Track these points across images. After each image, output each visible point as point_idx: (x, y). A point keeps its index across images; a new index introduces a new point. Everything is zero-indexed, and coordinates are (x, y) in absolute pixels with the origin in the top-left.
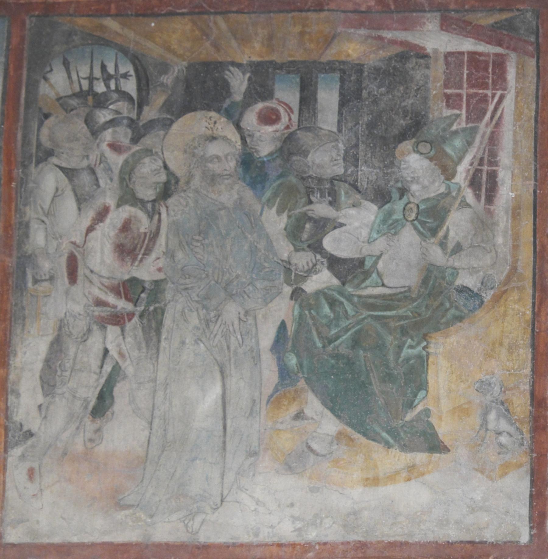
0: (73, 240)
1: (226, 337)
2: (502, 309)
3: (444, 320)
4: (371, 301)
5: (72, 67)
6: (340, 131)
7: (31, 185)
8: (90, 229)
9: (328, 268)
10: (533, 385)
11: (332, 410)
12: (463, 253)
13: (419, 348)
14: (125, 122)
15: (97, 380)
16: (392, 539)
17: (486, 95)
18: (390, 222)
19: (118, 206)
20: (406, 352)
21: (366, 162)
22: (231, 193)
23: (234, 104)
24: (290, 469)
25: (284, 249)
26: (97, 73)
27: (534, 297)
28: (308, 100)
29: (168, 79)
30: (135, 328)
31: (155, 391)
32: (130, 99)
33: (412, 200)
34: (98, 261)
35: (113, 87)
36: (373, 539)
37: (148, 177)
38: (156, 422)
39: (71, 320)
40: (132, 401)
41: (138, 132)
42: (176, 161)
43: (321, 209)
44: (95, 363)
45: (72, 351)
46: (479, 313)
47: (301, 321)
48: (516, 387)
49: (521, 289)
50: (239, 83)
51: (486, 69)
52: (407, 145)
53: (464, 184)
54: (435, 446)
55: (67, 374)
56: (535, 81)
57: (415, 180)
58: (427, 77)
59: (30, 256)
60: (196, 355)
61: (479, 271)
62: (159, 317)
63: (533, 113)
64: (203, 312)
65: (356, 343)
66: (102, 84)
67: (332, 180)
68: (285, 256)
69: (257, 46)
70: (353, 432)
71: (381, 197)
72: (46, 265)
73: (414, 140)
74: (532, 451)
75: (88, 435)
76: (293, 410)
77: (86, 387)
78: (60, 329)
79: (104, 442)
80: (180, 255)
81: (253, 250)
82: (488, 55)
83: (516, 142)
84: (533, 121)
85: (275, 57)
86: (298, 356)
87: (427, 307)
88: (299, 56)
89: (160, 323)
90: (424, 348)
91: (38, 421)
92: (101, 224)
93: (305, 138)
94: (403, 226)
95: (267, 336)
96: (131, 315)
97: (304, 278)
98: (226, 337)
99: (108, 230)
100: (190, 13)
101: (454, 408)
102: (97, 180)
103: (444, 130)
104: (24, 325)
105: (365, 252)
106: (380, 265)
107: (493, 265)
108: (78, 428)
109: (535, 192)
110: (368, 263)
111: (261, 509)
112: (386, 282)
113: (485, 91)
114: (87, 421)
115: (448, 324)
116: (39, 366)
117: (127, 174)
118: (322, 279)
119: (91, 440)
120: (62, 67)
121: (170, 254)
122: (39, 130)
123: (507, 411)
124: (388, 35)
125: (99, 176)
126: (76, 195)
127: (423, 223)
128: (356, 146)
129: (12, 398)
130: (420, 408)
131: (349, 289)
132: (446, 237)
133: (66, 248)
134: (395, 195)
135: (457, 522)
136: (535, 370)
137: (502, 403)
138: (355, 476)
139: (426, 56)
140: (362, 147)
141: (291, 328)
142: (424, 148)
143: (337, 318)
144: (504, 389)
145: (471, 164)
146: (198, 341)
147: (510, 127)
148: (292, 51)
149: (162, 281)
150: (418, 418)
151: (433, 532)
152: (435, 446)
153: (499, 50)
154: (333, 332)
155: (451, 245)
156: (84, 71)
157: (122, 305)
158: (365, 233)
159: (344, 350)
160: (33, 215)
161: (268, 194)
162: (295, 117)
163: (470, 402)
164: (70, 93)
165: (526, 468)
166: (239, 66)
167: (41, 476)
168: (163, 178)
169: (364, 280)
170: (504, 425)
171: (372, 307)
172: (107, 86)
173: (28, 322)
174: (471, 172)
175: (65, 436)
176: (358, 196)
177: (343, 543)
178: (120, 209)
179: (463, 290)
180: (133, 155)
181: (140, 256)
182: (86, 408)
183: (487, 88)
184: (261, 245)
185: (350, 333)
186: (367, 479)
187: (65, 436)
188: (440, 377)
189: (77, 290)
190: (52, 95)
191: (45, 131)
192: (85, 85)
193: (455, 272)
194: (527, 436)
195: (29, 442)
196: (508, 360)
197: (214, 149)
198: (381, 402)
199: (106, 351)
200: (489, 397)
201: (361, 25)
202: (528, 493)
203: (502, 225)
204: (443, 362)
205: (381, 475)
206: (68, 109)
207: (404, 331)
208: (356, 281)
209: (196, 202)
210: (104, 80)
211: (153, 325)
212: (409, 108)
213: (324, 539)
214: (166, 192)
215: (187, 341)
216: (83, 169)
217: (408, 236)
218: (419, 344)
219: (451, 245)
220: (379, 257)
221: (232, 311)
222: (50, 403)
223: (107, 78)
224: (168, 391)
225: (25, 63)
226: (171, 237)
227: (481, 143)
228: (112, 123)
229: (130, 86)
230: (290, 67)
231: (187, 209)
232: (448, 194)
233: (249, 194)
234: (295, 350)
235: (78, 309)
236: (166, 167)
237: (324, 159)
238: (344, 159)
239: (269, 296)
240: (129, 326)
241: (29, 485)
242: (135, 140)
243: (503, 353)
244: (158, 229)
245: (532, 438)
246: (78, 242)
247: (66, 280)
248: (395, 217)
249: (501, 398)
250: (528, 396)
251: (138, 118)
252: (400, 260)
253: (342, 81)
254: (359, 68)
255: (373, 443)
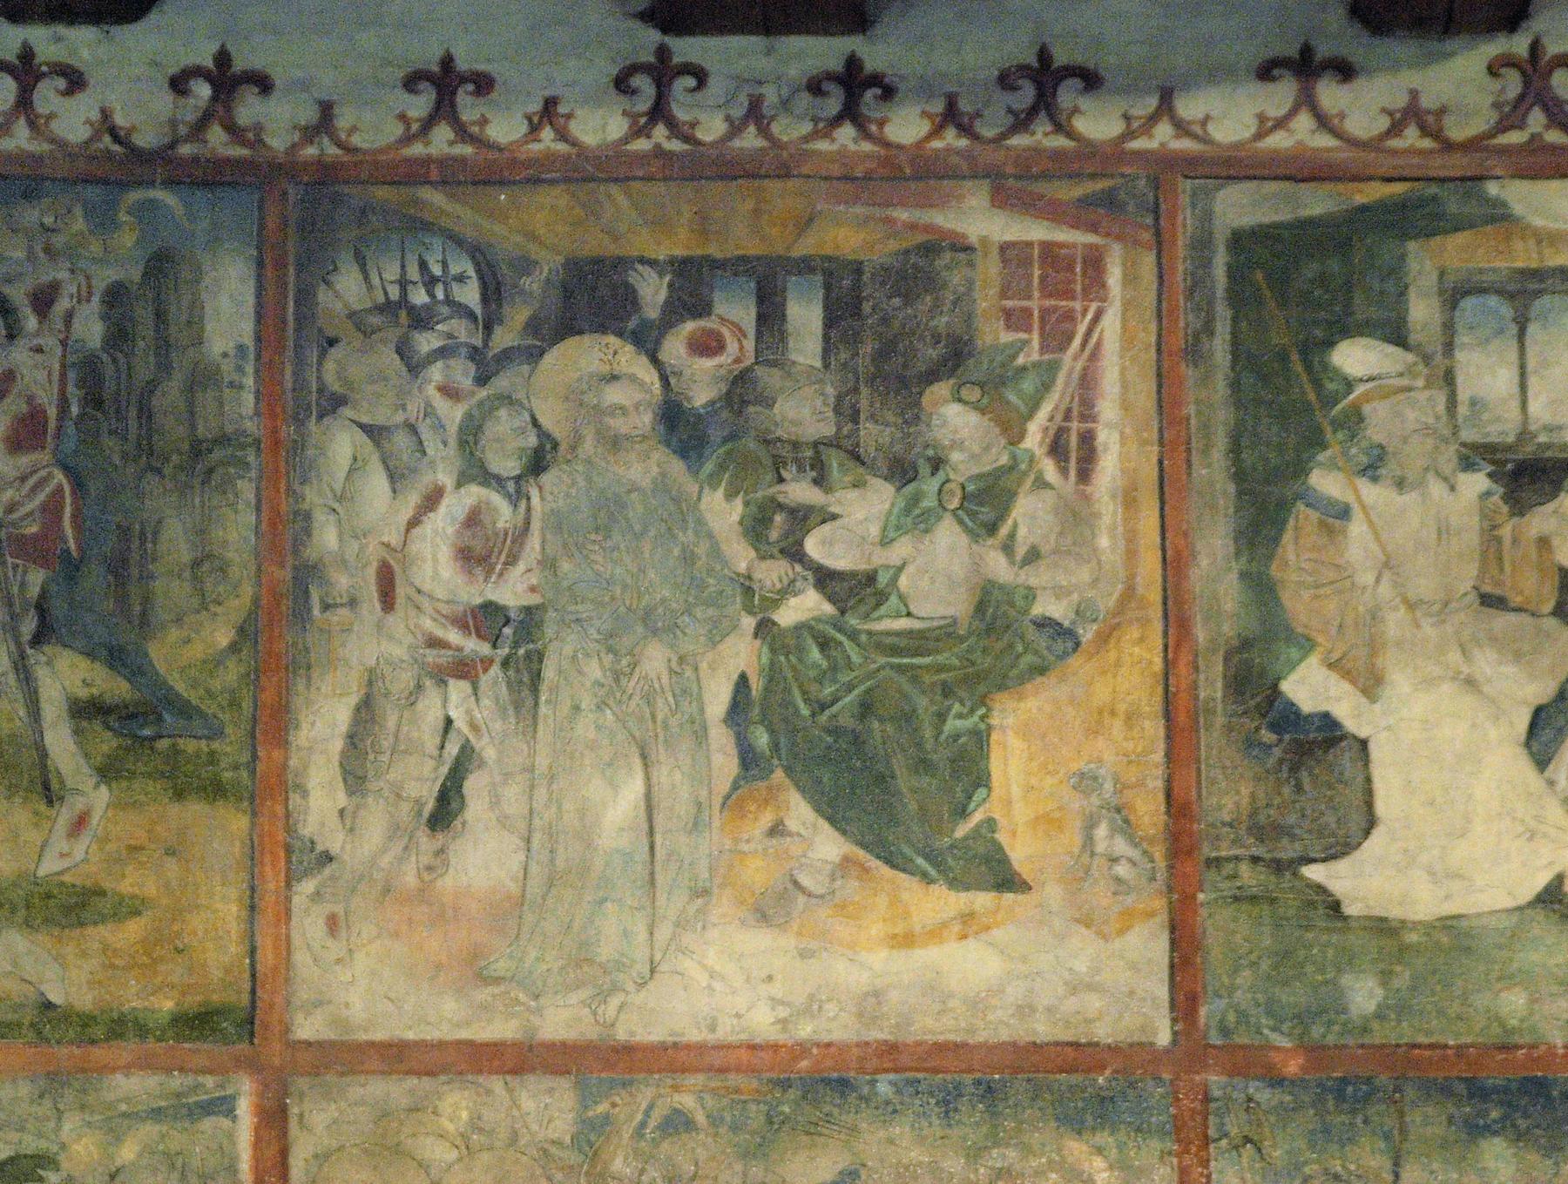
0: (385, 539)
1: (649, 699)
2: (1112, 655)
3: (1015, 672)
4: (889, 640)
5: (370, 264)
6: (826, 366)
7: (310, 452)
8: (414, 523)
9: (815, 586)
10: (1169, 781)
11: (831, 820)
12: (1043, 563)
13: (976, 718)
14: (464, 351)
15: (436, 769)
16: (941, 1038)
17: (1072, 310)
18: (917, 511)
19: (459, 485)
20: (952, 725)
21: (872, 416)
22: (648, 466)
23: (646, 325)
24: (763, 916)
25: (741, 556)
26: (413, 273)
27: (1166, 634)
28: (770, 317)
29: (532, 284)
30: (495, 683)
31: (532, 787)
32: (471, 315)
33: (952, 476)
34: (429, 572)
35: (440, 295)
36: (910, 1040)
37: (505, 450)
38: (537, 839)
39: (387, 670)
40: (496, 801)
41: (486, 367)
42: (552, 417)
43: (800, 491)
44: (431, 742)
45: (391, 723)
46: (1075, 661)
47: (772, 674)
48: (1141, 784)
49: (1145, 622)
50: (653, 291)
51: (1070, 268)
52: (942, 389)
53: (1039, 452)
54: (1006, 880)
55: (385, 758)
56: (1155, 286)
57: (957, 445)
58: (970, 283)
59: (314, 567)
60: (598, 728)
61: (1070, 593)
62: (535, 666)
63: (1153, 339)
64: (608, 659)
65: (866, 708)
66: (423, 291)
67: (816, 444)
68: (742, 567)
69: (683, 233)
70: (868, 856)
71: (901, 472)
72: (342, 582)
73: (952, 381)
74: (1170, 889)
75: (425, 860)
76: (767, 819)
77: (418, 779)
78: (370, 683)
79: (451, 870)
80: (565, 566)
81: (688, 558)
82: (1074, 246)
83: (1125, 385)
84: (1153, 350)
85: (714, 250)
86: (772, 732)
87: (985, 650)
88: (753, 248)
89: (537, 677)
90: (982, 718)
91: (341, 836)
92: (431, 515)
93: (769, 378)
94: (940, 518)
95: (718, 699)
96: (487, 663)
97: (776, 603)
98: (649, 699)
99: (444, 522)
100: (567, 180)
101: (1037, 818)
102: (421, 442)
103: (1003, 365)
104: (309, 678)
105: (877, 561)
106: (903, 581)
107: (1095, 582)
108: (406, 848)
109: (1160, 462)
110: (883, 579)
111: (717, 985)
112: (912, 608)
113: (1071, 304)
114: (423, 836)
115: (1022, 680)
116: (338, 745)
117: (470, 435)
118: (806, 605)
119: (429, 868)
120: (356, 267)
121: (548, 564)
122: (320, 364)
123: (1125, 825)
124: (902, 215)
125: (423, 437)
126: (387, 468)
127: (973, 515)
128: (856, 390)
129: (295, 799)
130: (978, 817)
131: (853, 621)
132: (1012, 536)
133: (374, 553)
134: (925, 469)
135: (1050, 1010)
136: (1169, 756)
137: (1118, 811)
138: (873, 932)
139: (968, 249)
140: (865, 391)
141: (756, 685)
142: (971, 394)
143: (834, 668)
144: (1121, 787)
145: (1051, 419)
146: (601, 706)
147: (1115, 359)
148: (741, 240)
149: (537, 607)
150: (976, 833)
151: (1007, 1025)
152: (1006, 880)
153: (1091, 238)
154: (828, 690)
155: (1021, 551)
156: (392, 272)
157: (473, 646)
158: (874, 530)
159: (847, 721)
160: (318, 500)
161: (709, 467)
162: (750, 344)
163: (1060, 808)
164: (369, 305)
165: (1162, 918)
166: (652, 263)
167: (348, 927)
168: (532, 440)
169: (878, 605)
170: (1121, 846)
171: (895, 651)
172: (432, 295)
173: (315, 675)
174: (1052, 432)
175: (385, 861)
176: (861, 470)
177: (858, 1045)
178: (462, 490)
179: (1044, 623)
180: (481, 404)
181: (499, 567)
182: (419, 813)
183: (1073, 298)
184: (702, 549)
185: (856, 692)
186: (895, 936)
187: (385, 861)
188: (1012, 764)
189: (395, 621)
190: (339, 306)
191: (330, 366)
192: (394, 293)
193: (1031, 595)
194: (1161, 864)
195: (327, 871)
196: (1126, 739)
197: (614, 395)
198: (913, 806)
199: (449, 722)
200: (1095, 800)
201: (856, 200)
202: (1167, 960)
203: (1106, 520)
204: (1015, 743)
205: (918, 928)
206: (366, 332)
207: (947, 691)
208: (863, 609)
209: (589, 480)
210: (425, 285)
211: (526, 679)
212: (942, 330)
213: (826, 1038)
214: (537, 464)
215: (583, 706)
216: (397, 426)
217: (948, 536)
218: (972, 711)
219: (1021, 551)
220: (900, 569)
221: (656, 659)
222: (358, 807)
223: (430, 282)
224: (554, 786)
225: (291, 259)
226: (549, 537)
227: (1067, 384)
228: (442, 353)
229: (470, 294)
230: (740, 266)
231: (573, 492)
232: (1012, 468)
233: (677, 466)
234: (765, 720)
235: (398, 652)
236: (535, 423)
237: (802, 411)
238: (837, 410)
239: (718, 633)
240: (485, 680)
241: (330, 942)
242: (482, 380)
243: (1118, 725)
244: (527, 522)
245: (1171, 867)
246: (394, 543)
247: (378, 606)
248: (925, 504)
249: (1114, 801)
250: (1161, 797)
251: (486, 345)
252: (936, 574)
253: (828, 287)
254: (857, 268)
255: (902, 875)
